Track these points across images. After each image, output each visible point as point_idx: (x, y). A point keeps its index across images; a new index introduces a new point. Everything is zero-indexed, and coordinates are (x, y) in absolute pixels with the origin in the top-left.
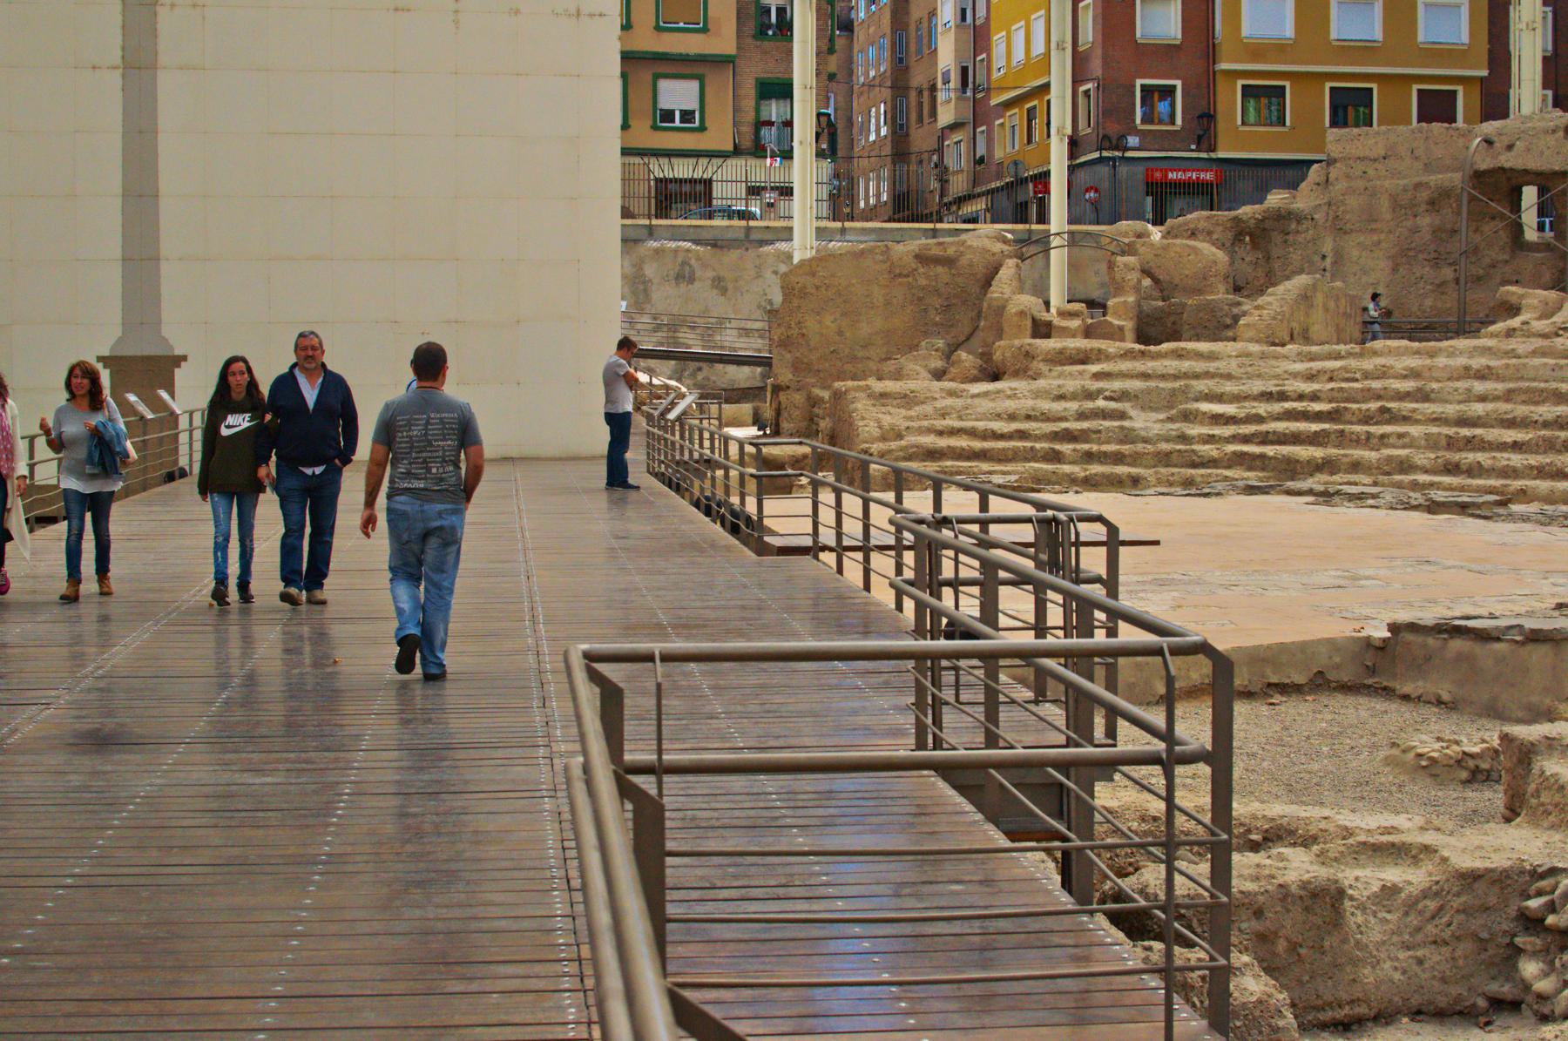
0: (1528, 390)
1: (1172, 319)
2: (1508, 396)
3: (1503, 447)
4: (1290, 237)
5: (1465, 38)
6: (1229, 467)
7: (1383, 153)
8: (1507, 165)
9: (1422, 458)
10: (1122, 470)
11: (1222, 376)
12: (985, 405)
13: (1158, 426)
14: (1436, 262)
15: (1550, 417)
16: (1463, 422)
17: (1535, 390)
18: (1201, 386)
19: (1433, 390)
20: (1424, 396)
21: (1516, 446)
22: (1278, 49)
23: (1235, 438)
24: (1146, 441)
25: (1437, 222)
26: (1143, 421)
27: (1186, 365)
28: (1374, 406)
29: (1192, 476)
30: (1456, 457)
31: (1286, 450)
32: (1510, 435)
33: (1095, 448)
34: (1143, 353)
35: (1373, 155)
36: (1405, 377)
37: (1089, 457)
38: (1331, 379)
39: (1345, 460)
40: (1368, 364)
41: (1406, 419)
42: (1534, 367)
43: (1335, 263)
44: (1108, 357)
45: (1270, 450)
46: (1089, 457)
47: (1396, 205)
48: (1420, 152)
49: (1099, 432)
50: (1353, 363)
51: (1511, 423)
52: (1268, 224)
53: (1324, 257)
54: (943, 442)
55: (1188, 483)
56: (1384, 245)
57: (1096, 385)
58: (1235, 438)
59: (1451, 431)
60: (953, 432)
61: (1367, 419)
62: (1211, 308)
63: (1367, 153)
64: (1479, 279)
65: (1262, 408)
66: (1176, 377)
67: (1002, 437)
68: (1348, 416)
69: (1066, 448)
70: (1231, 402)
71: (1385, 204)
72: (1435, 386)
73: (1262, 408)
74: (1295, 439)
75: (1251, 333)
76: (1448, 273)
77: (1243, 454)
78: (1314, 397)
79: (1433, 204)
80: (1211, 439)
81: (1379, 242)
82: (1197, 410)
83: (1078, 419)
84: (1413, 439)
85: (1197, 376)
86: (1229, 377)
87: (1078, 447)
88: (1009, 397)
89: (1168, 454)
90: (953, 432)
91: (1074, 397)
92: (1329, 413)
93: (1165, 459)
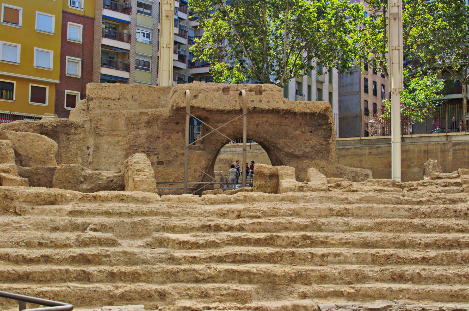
0: (391, 224)
1: (38, 177)
2: (378, 227)
3: (415, 261)
4: (71, 137)
5: (52, 67)
6: (224, 282)
7: (118, 96)
8: (196, 105)
9: (369, 270)
11: (163, 214)
13: (148, 250)
15: (428, 241)
16: (366, 244)
17: (396, 223)
18: (155, 220)
19: (323, 224)
20: (320, 229)
21: (424, 260)
23: (211, 259)
24: (145, 262)
25: (150, 133)
27: (133, 206)
28: (298, 234)
29: (206, 290)
31: (263, 267)
33: (116, 269)
34: (95, 197)
35: (113, 97)
36: (291, 215)
37: (112, 277)
38: (239, 217)
39: (313, 274)
40: (264, 206)
41: (323, 243)
42: (378, 209)
43: (95, 151)
44: (68, 201)
46: (112, 277)
47: (129, 122)
48: (136, 98)
49: (108, 256)
50: (247, 205)
51: (403, 245)
52: (58, 129)
53: (88, 148)
56: (121, 143)
57: (80, 220)
59: (373, 251)
61: (294, 244)
62: (73, 172)
63: (110, 96)
64: (170, 162)
65: (212, 237)
66: (130, 215)
67: (30, 261)
68: (279, 242)
69: (91, 269)
70: (181, 232)
71: (122, 122)
72: (323, 220)
73: (212, 237)
74: (257, 259)
75: (145, 186)
77: (234, 271)
78: (241, 228)
80: (194, 260)
81: (118, 142)
82: (168, 238)
83: (79, 246)
84: (346, 257)
85: (145, 214)
86: (169, 215)
87: (102, 268)
88: (16, 229)
89: (175, 273)
91: (65, 229)
92: (266, 240)
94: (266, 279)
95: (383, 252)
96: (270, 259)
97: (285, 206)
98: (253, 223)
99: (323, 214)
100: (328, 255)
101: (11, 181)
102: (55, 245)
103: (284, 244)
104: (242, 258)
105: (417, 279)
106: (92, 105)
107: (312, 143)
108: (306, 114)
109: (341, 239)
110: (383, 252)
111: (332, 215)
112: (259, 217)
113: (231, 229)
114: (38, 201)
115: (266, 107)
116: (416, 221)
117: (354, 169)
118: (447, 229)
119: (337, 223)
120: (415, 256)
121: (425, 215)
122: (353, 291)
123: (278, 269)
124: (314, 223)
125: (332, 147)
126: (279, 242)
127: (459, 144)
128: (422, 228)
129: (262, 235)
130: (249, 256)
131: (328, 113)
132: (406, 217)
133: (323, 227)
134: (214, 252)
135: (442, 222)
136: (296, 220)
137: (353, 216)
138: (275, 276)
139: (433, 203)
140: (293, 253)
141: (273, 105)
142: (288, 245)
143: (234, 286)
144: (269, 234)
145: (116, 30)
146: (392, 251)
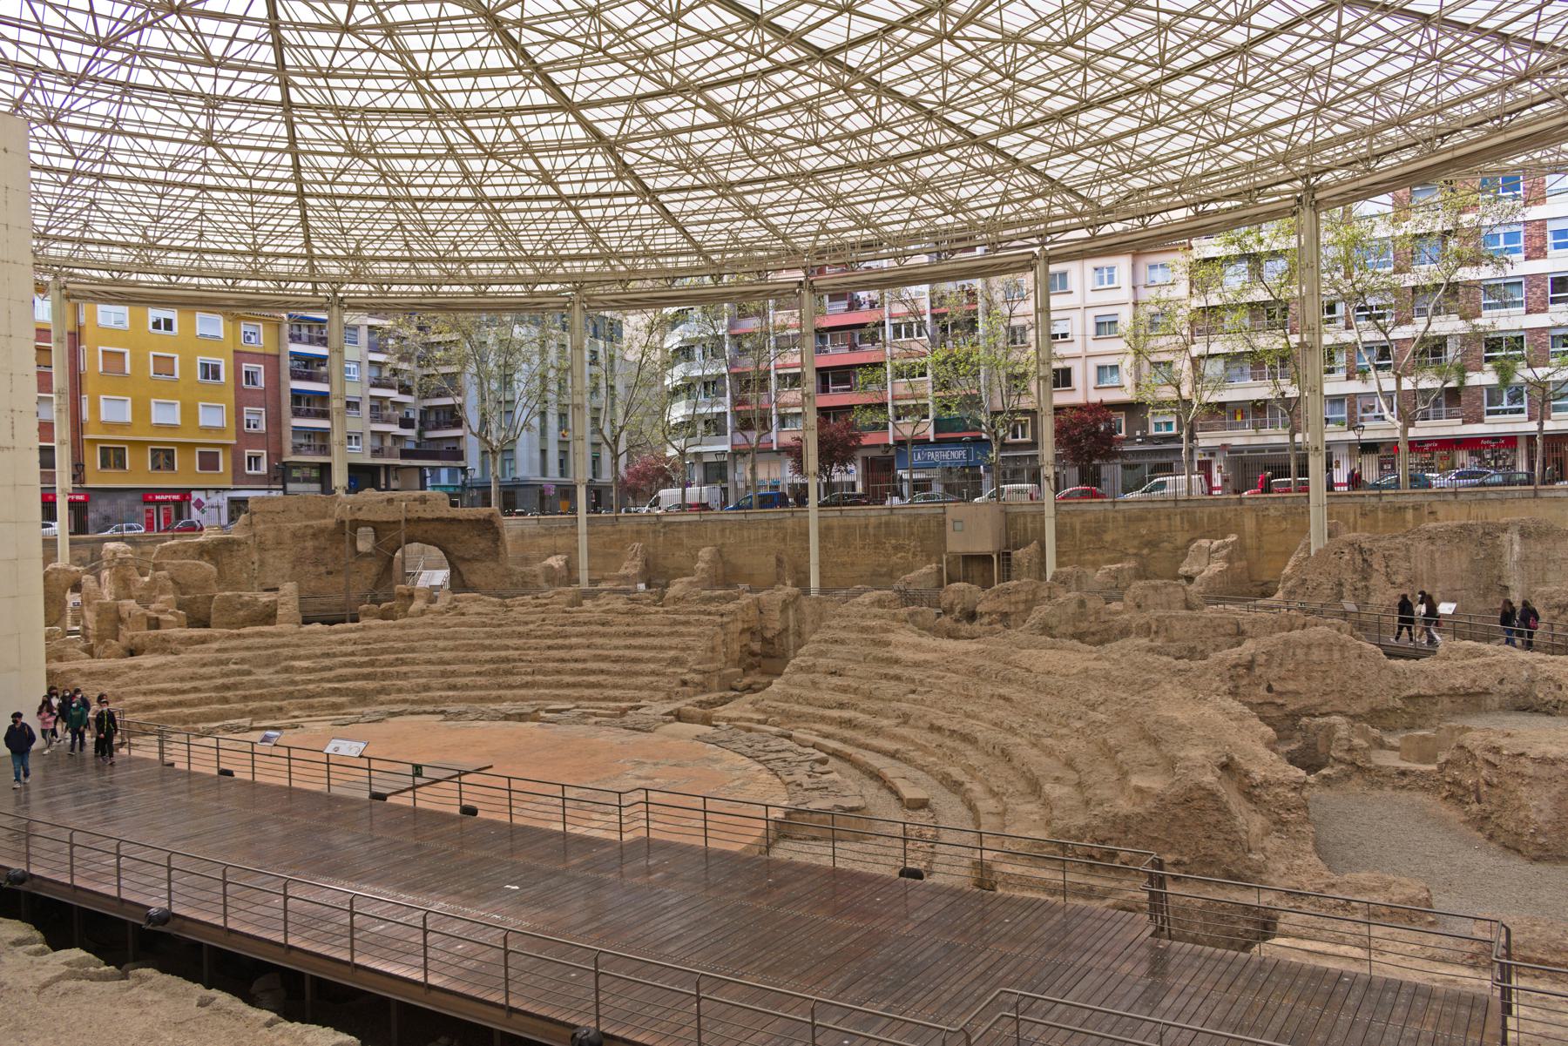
2: (456, 648)
3: (471, 674)
9: (434, 682)
10: (268, 703)
12: (162, 675)
14: (316, 564)
16: (442, 662)
18: (286, 652)
20: (413, 650)
21: (479, 674)
22: (122, 426)
23: (322, 680)
26: (263, 675)
27: (270, 641)
30: (451, 680)
31: (359, 683)
32: (476, 669)
37: (245, 698)
40: (373, 634)
44: (216, 639)
45: (351, 684)
46: (245, 698)
47: (294, 535)
54: (153, 699)
55: (311, 707)
57: (225, 656)
58: (322, 680)
60: (152, 692)
61: (391, 664)
65: (327, 662)
66: (266, 648)
67: (184, 692)
69: (229, 694)
71: (287, 535)
73: (327, 662)
76: (322, 569)
78: (353, 654)
79: (315, 536)
80: (310, 681)
86: (298, 646)
90: (152, 692)
91: (211, 664)
93: (290, 695)
95: (449, 668)
101: (170, 624)
102: (202, 678)
106: (255, 519)
107: (481, 546)
110: (449, 668)
113: (346, 655)
114: (190, 641)
115: (430, 516)
116: (487, 642)
118: (507, 648)
123: (371, 685)
128: (490, 648)
134: (326, 674)
141: (437, 514)
143: (334, 699)
145: (308, 367)
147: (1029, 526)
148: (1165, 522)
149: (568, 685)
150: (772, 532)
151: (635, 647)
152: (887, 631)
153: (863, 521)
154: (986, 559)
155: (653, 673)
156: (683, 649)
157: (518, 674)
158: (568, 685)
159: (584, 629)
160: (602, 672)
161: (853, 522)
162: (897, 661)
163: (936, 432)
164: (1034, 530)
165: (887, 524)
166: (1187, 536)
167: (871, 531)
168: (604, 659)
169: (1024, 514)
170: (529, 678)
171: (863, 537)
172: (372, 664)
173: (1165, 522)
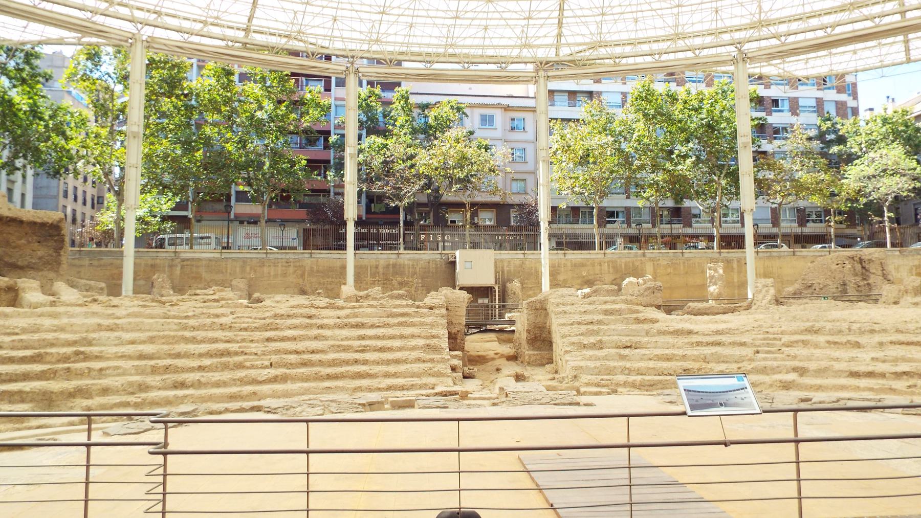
2: (152, 340)
3: (192, 370)
9: (150, 380)
15: (202, 351)
16: (142, 357)
19: (94, 339)
20: (90, 343)
21: (201, 368)
32: (195, 363)
36: (55, 331)
39: (94, 387)
41: (98, 358)
51: (178, 356)
59: (152, 363)
68: (48, 358)
74: (26, 377)
84: (125, 370)
92: (32, 357)
94: (41, 397)
96: (41, 376)
97: (47, 322)
98: (13, 341)
99: (91, 329)
100: (108, 368)
103: (53, 360)
104: (8, 378)
105: (199, 384)
108: (35, 223)
109: (116, 353)
111: (101, 330)
112: (17, 334)
116: (187, 334)
117: (88, 282)
118: (215, 341)
119: (109, 338)
120: (192, 365)
121: (194, 328)
122: (139, 400)
124: (85, 339)
125: (64, 259)
126: (48, 358)
127: (188, 260)
128: (194, 340)
129: (28, 353)
130: (16, 375)
131: (62, 225)
132: (176, 330)
133: (94, 342)
135: (210, 334)
136: (63, 336)
137: (123, 330)
138: (52, 392)
139: (199, 318)
140: (69, 368)
142: (59, 361)
144: (36, 351)
146: (168, 362)
147: (506, 269)
148: (597, 268)
149: (329, 377)
150: (291, 270)
151: (370, 338)
152: (638, 312)
153: (373, 262)
154: (485, 291)
155: (419, 360)
156: (427, 338)
157: (253, 367)
158: (329, 377)
159: (295, 321)
160: (356, 362)
161: (366, 262)
162: (690, 332)
163: (367, 213)
164: (509, 272)
165: (394, 265)
166: (612, 277)
167: (381, 270)
168: (346, 349)
169: (502, 260)
170: (273, 372)
171: (373, 275)
172: (36, 359)
173: (597, 268)
